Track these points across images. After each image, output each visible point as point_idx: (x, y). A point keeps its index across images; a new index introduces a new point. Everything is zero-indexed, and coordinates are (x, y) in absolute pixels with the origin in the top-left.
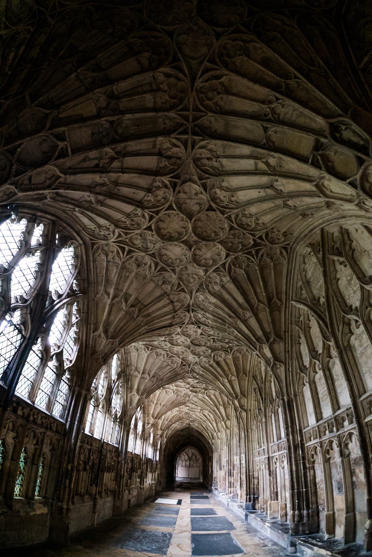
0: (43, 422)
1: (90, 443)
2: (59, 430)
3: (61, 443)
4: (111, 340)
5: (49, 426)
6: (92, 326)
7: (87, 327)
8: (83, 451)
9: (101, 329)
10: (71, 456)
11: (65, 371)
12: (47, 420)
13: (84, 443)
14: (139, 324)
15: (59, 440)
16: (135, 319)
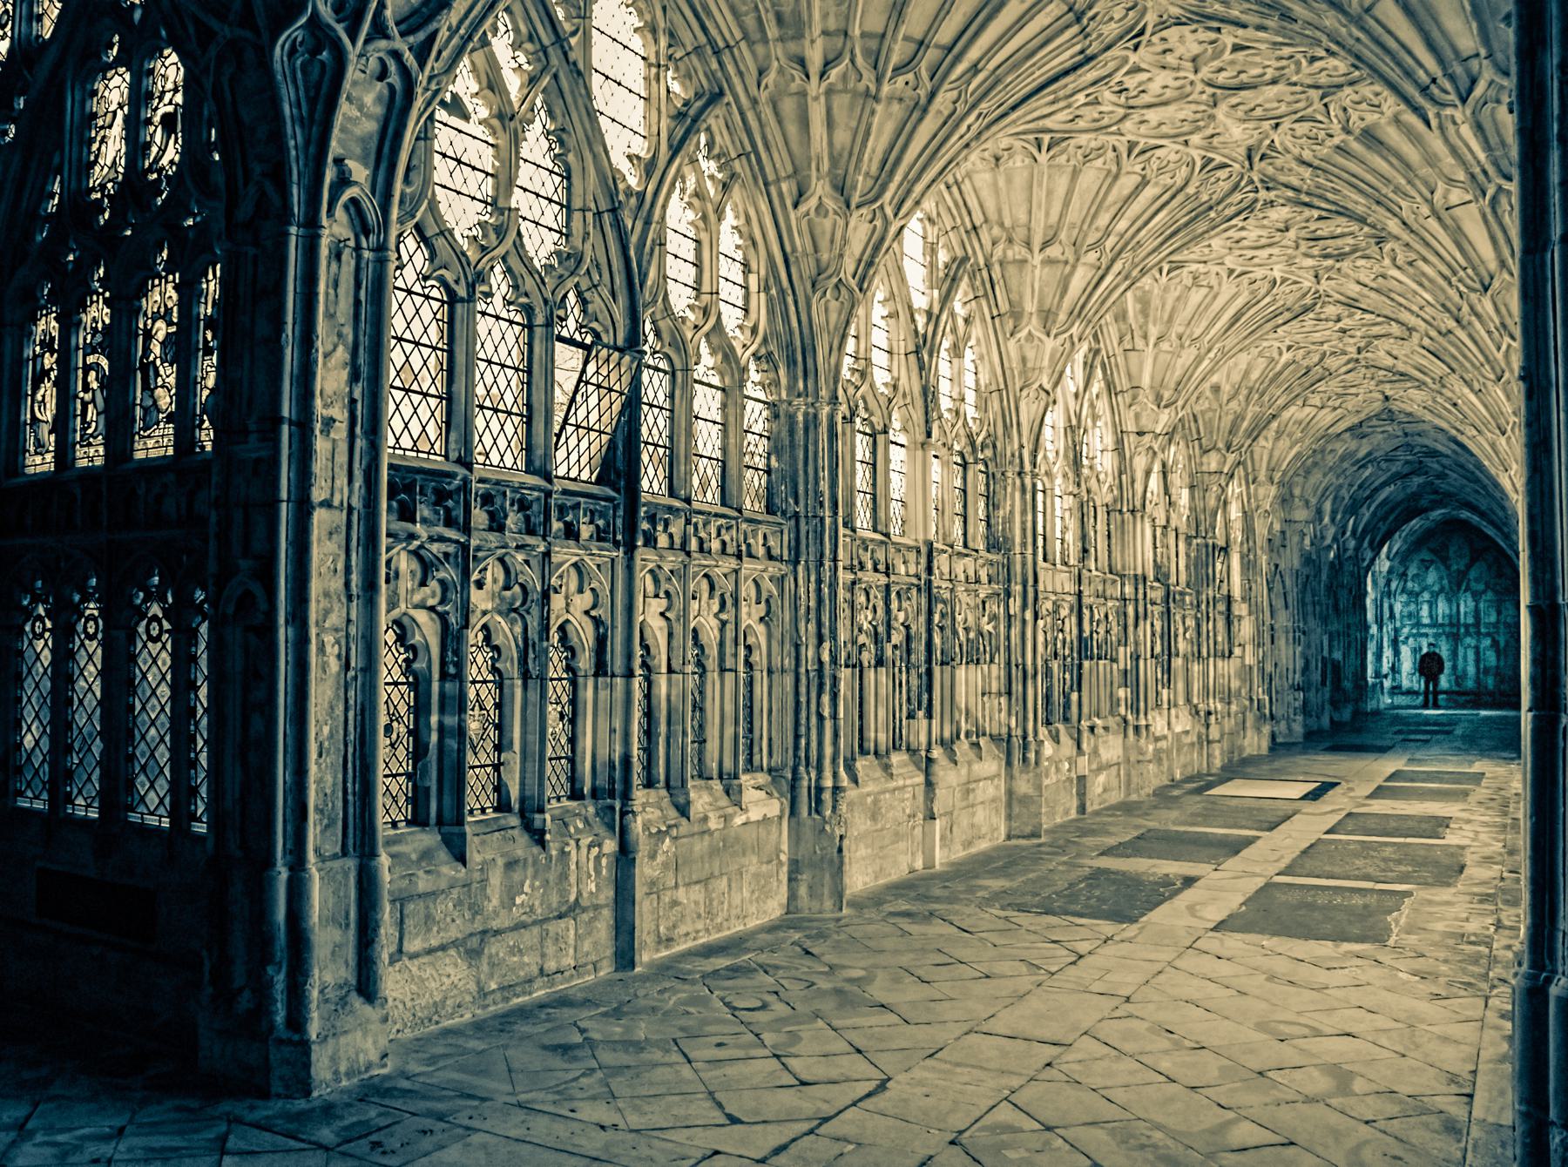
0: (724, 543)
1: (881, 567)
2: (776, 552)
3: (789, 583)
4: (864, 211)
5: (744, 548)
6: (784, 186)
7: (769, 195)
8: (863, 599)
9: (820, 189)
10: (826, 620)
11: (745, 370)
12: (734, 532)
13: (862, 567)
14: (946, 113)
15: (780, 581)
16: (925, 111)
